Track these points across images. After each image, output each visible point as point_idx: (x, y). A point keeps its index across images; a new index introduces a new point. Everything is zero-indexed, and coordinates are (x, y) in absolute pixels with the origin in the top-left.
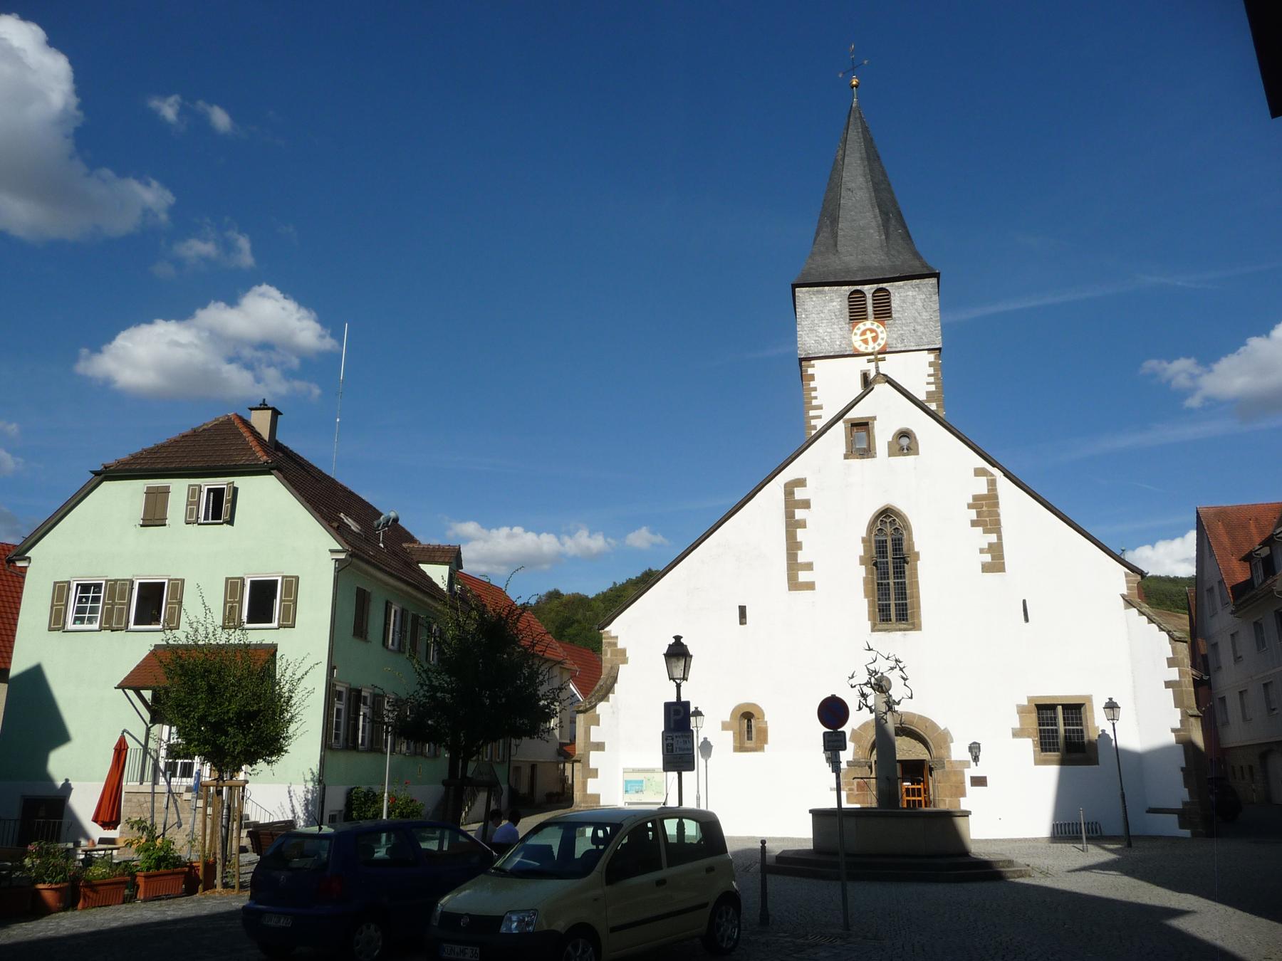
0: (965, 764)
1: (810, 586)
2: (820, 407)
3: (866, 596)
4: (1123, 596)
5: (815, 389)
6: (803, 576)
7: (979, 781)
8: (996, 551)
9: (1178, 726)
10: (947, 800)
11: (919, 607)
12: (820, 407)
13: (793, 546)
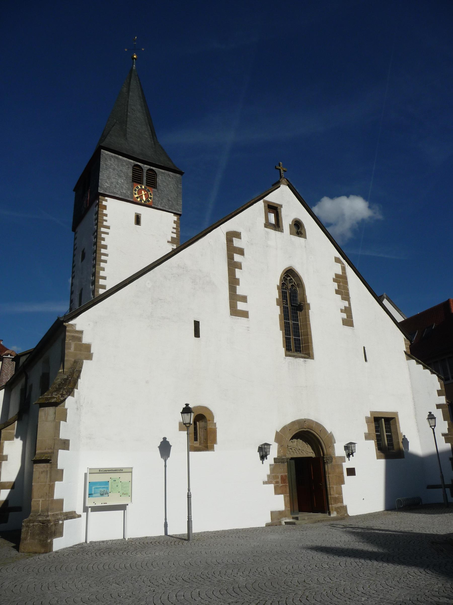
0: (342, 459)
2: (108, 227)
3: (281, 329)
4: (405, 351)
5: (106, 215)
6: (241, 306)
7: (351, 472)
9: (446, 432)
10: (335, 487)
11: (312, 343)
12: (108, 227)
13: (233, 282)
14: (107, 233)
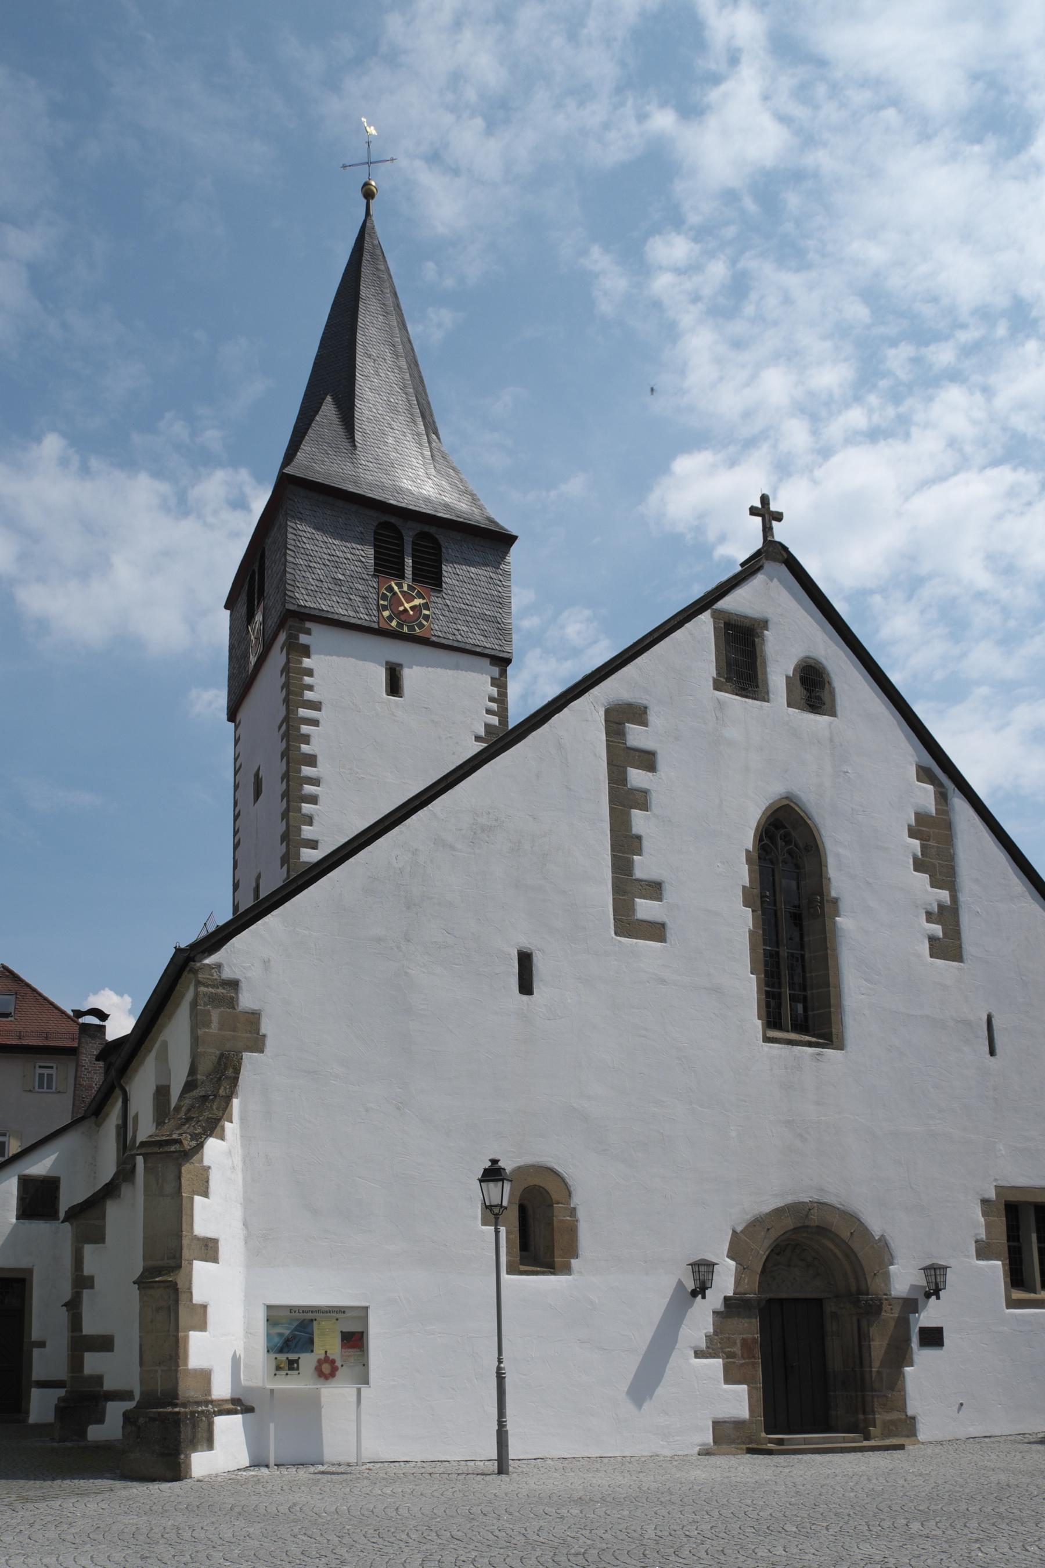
1: (656, 931)
2: (316, 706)
5: (310, 673)
6: (645, 909)
7: (933, 1337)
8: (947, 916)
13: (625, 845)
14: (315, 723)
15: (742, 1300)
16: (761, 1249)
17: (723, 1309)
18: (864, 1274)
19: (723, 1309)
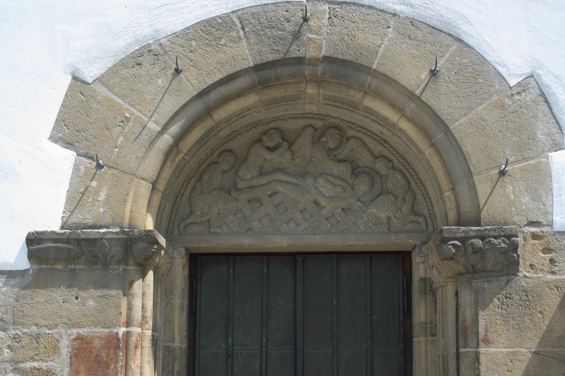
15: (78, 241)
16: (152, 119)
17: (24, 264)
18: (470, 174)
19: (24, 264)
